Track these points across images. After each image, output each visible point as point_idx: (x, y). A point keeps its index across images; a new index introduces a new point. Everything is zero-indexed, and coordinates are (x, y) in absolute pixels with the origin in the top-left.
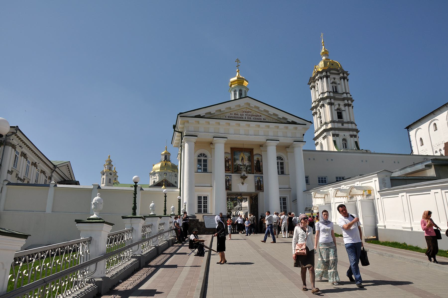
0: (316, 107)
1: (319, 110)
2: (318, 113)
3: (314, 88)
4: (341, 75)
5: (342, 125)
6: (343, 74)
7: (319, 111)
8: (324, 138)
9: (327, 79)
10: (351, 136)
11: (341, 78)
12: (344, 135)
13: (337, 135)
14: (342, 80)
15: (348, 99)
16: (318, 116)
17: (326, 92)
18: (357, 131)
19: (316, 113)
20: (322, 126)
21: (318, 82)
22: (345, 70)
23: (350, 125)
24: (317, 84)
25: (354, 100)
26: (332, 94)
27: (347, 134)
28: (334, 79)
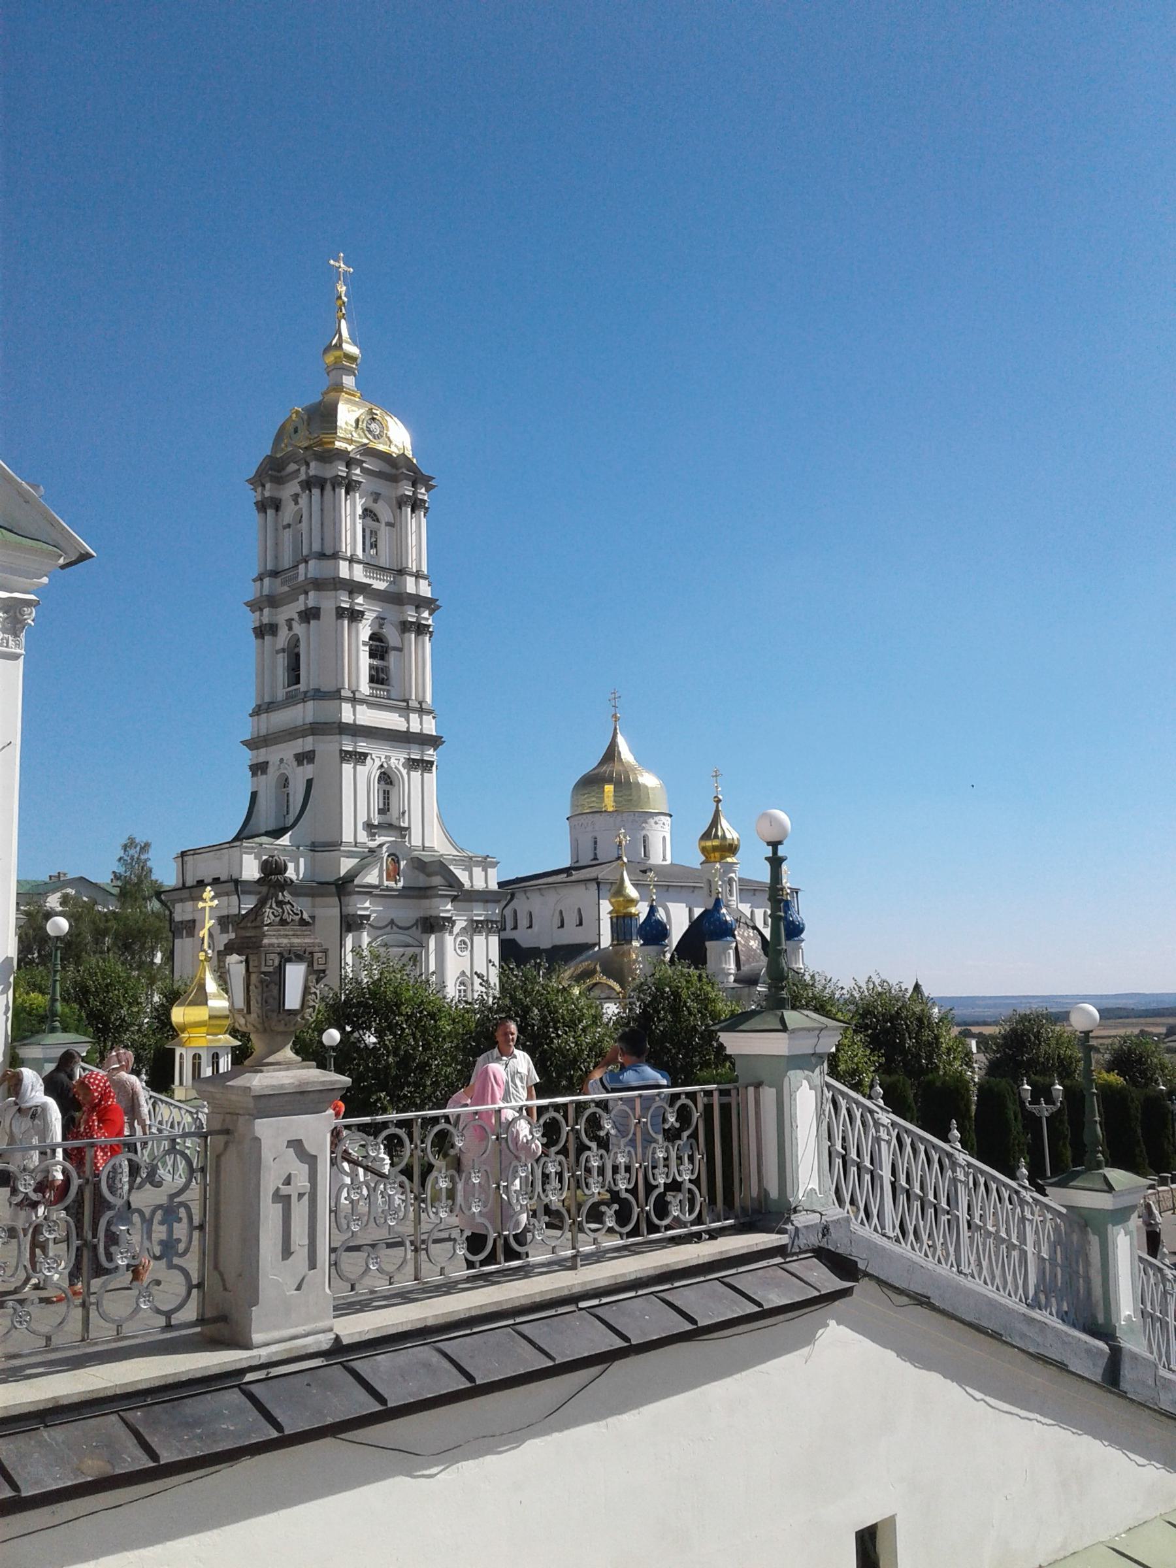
0: (272, 601)
1: (289, 622)
2: (283, 635)
3: (277, 508)
7: (290, 629)
9: (347, 493)
10: (413, 764)
11: (401, 502)
12: (388, 758)
13: (361, 758)
15: (420, 602)
18: (434, 741)
20: (292, 699)
24: (296, 498)
25: (439, 607)
26: (359, 574)
28: (376, 497)
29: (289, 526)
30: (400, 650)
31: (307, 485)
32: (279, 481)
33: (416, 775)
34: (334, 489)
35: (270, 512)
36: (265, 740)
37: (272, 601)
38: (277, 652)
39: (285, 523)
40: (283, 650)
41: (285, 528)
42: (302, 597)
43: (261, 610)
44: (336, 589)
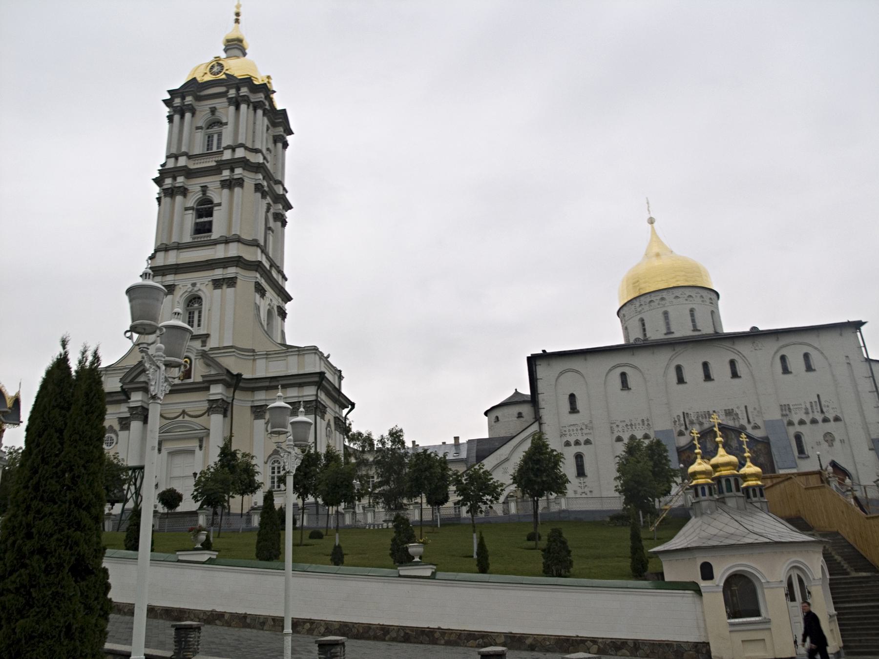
0: (189, 173)
1: (204, 189)
3: (193, 114)
4: (280, 130)
5: (271, 266)
6: (285, 131)
8: (217, 284)
14: (280, 145)
16: (191, 201)
17: (257, 151)
19: (184, 191)
21: (232, 109)
22: (293, 126)
23: (280, 277)
24: (213, 111)
27: (276, 301)
29: (200, 128)
30: (273, 232)
31: (236, 103)
32: (199, 99)
33: (279, 319)
34: (255, 110)
35: (188, 115)
36: (176, 269)
37: (189, 173)
38: (187, 209)
39: (199, 125)
40: (192, 208)
41: (198, 128)
42: (226, 173)
43: (175, 178)
44: (256, 172)
